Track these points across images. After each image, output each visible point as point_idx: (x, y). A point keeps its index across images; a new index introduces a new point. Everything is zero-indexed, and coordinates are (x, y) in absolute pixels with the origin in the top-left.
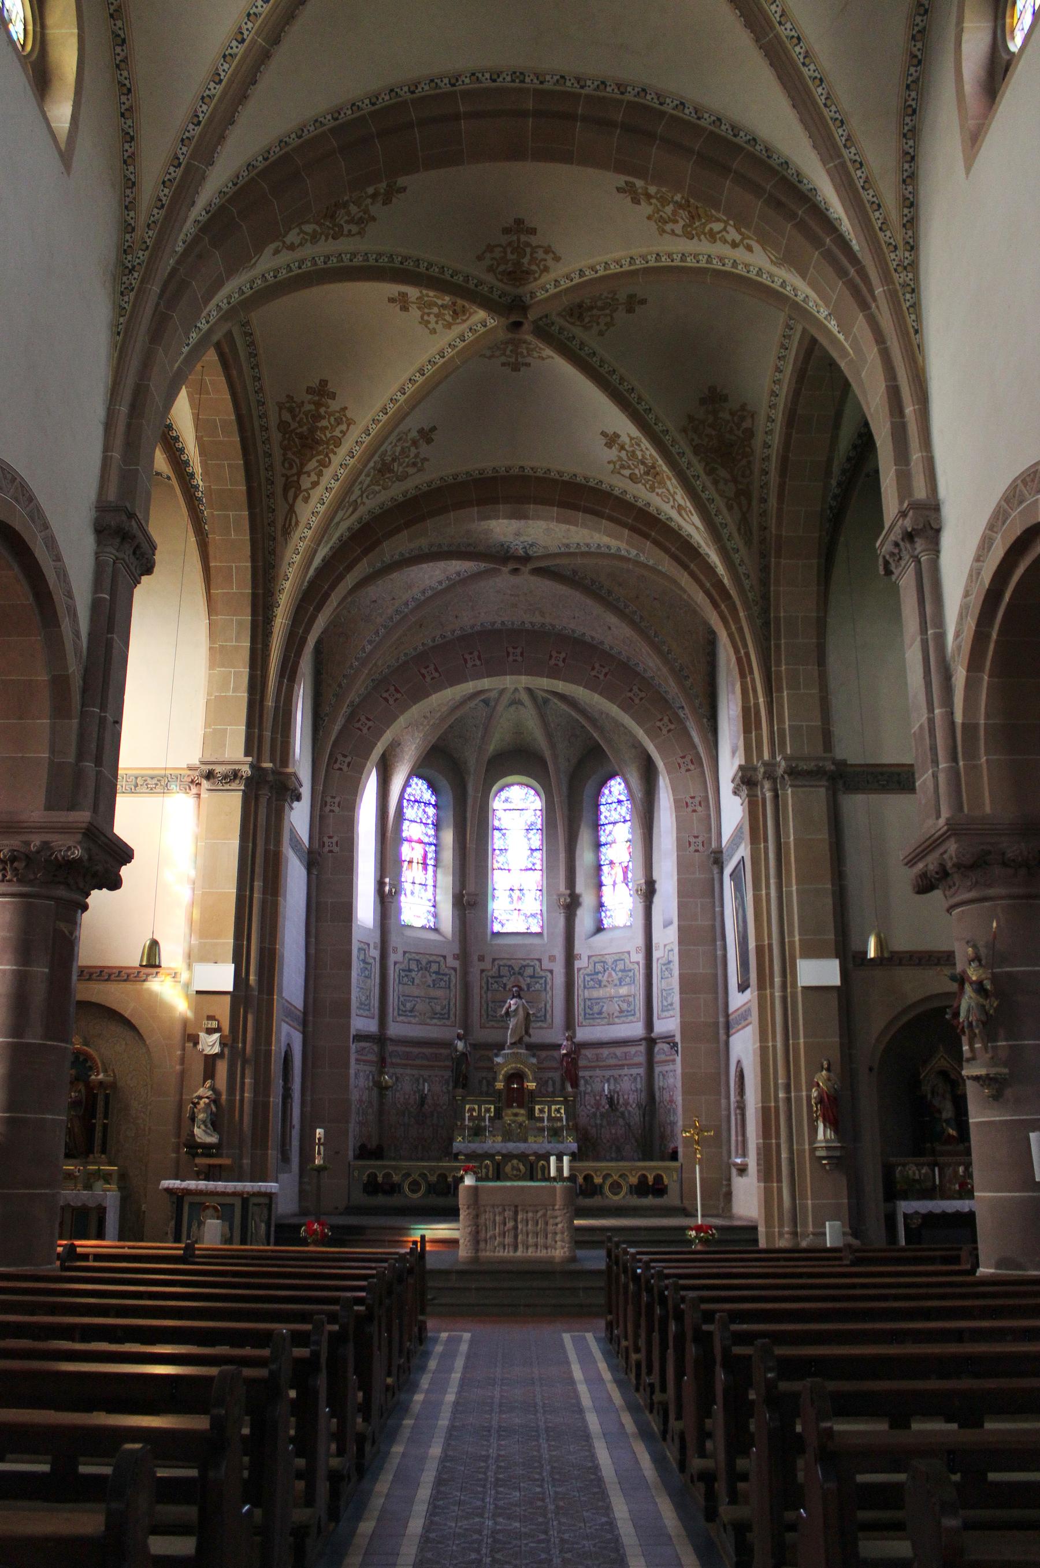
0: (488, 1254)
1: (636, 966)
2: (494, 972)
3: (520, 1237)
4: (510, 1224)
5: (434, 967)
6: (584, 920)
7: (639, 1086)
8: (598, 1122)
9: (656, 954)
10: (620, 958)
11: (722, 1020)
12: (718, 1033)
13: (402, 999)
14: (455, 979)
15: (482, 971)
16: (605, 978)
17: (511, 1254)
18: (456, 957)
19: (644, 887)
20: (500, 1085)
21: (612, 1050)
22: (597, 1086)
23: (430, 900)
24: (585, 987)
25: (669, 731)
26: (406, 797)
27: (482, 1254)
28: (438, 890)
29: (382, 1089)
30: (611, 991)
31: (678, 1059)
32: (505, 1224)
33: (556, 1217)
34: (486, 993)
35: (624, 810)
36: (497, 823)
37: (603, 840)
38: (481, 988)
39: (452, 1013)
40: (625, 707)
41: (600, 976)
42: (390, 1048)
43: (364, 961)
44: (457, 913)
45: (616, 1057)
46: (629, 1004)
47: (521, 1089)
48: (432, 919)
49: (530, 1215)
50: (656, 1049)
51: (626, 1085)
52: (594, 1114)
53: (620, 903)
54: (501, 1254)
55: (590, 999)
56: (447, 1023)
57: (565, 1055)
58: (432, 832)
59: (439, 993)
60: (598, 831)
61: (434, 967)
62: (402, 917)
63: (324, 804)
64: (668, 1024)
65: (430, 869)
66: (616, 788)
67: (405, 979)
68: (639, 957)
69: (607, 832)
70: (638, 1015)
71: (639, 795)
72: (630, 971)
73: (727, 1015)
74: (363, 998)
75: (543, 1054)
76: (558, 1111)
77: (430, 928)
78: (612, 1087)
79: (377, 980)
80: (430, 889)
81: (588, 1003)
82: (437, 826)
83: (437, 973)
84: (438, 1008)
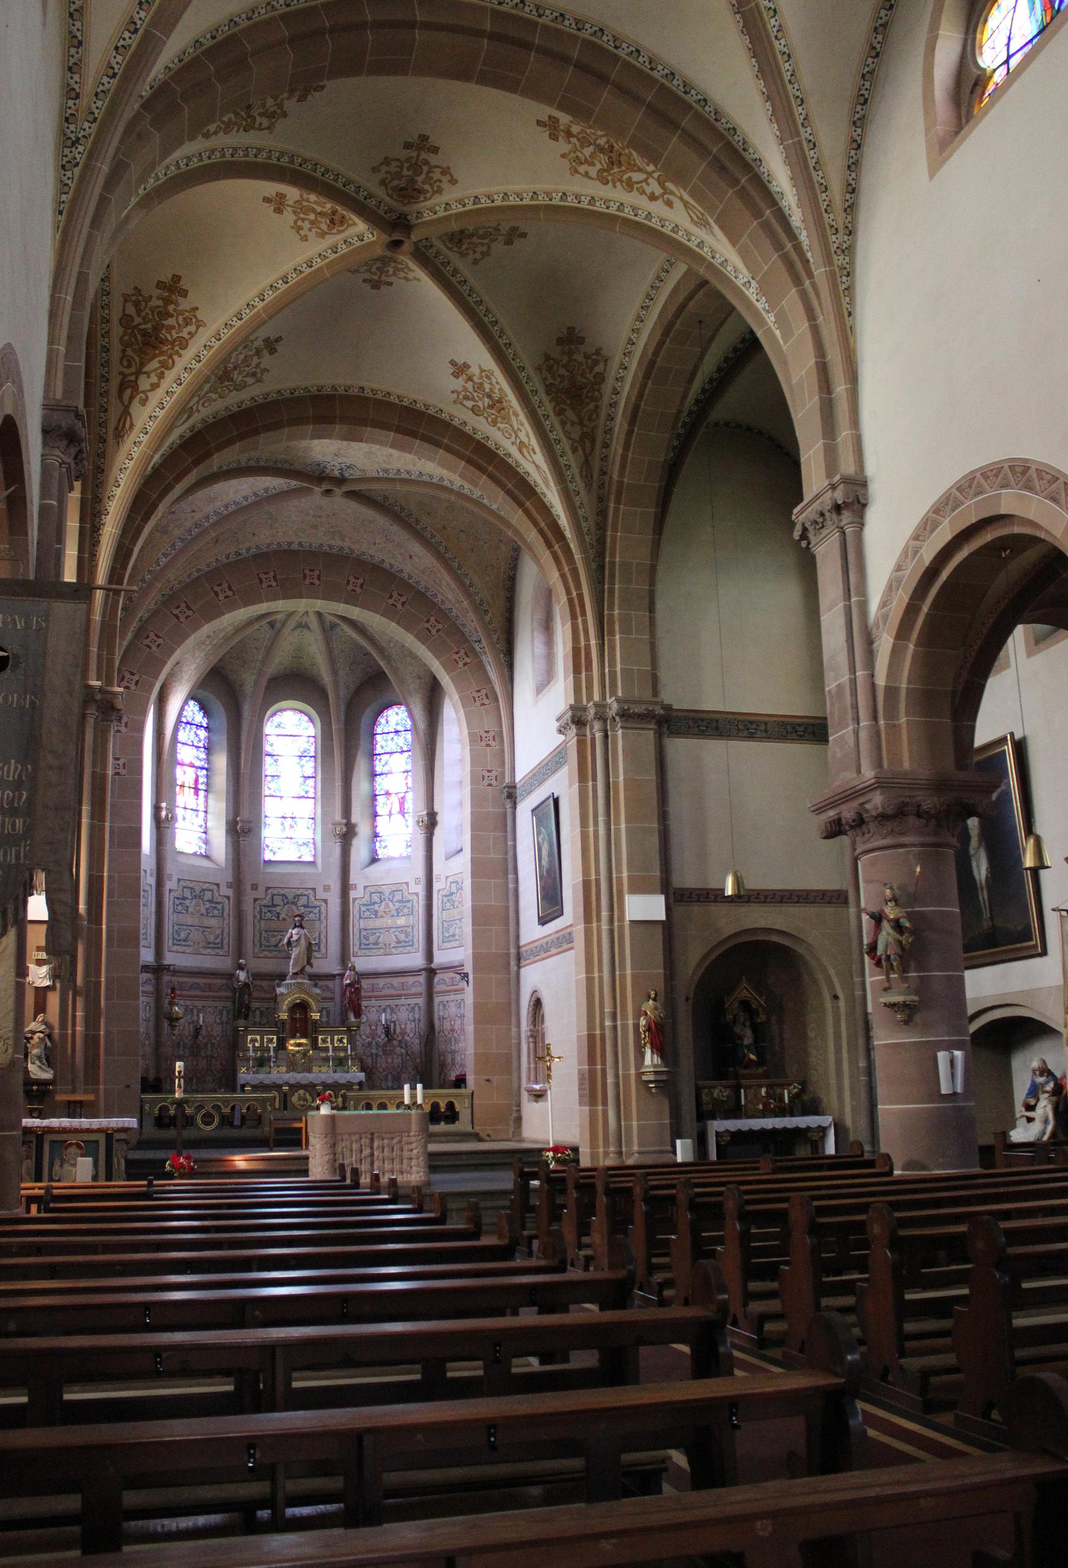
2: (267, 901)
4: (367, 1152)
5: (208, 895)
6: (360, 850)
7: (417, 1016)
8: (374, 1051)
9: (436, 886)
10: (397, 888)
11: (513, 951)
12: (509, 964)
14: (229, 908)
15: (255, 900)
18: (229, 885)
20: (284, 1016)
21: (389, 980)
23: (201, 826)
24: (360, 918)
25: (465, 664)
28: (209, 817)
30: (388, 921)
31: (469, 990)
32: (361, 1151)
35: (405, 739)
37: (379, 769)
38: (255, 917)
39: (225, 942)
40: (424, 637)
41: (376, 907)
44: (230, 840)
45: (393, 987)
46: (407, 935)
49: (386, 1141)
50: (436, 980)
51: (403, 1015)
52: (370, 1044)
58: (203, 756)
59: (212, 922)
61: (208, 895)
66: (395, 718)
69: (383, 762)
71: (422, 726)
72: (408, 901)
73: (518, 947)
76: (340, 1040)
78: (389, 1017)
79: (153, 909)
80: (202, 815)
81: (364, 933)
83: (211, 901)
84: (211, 938)
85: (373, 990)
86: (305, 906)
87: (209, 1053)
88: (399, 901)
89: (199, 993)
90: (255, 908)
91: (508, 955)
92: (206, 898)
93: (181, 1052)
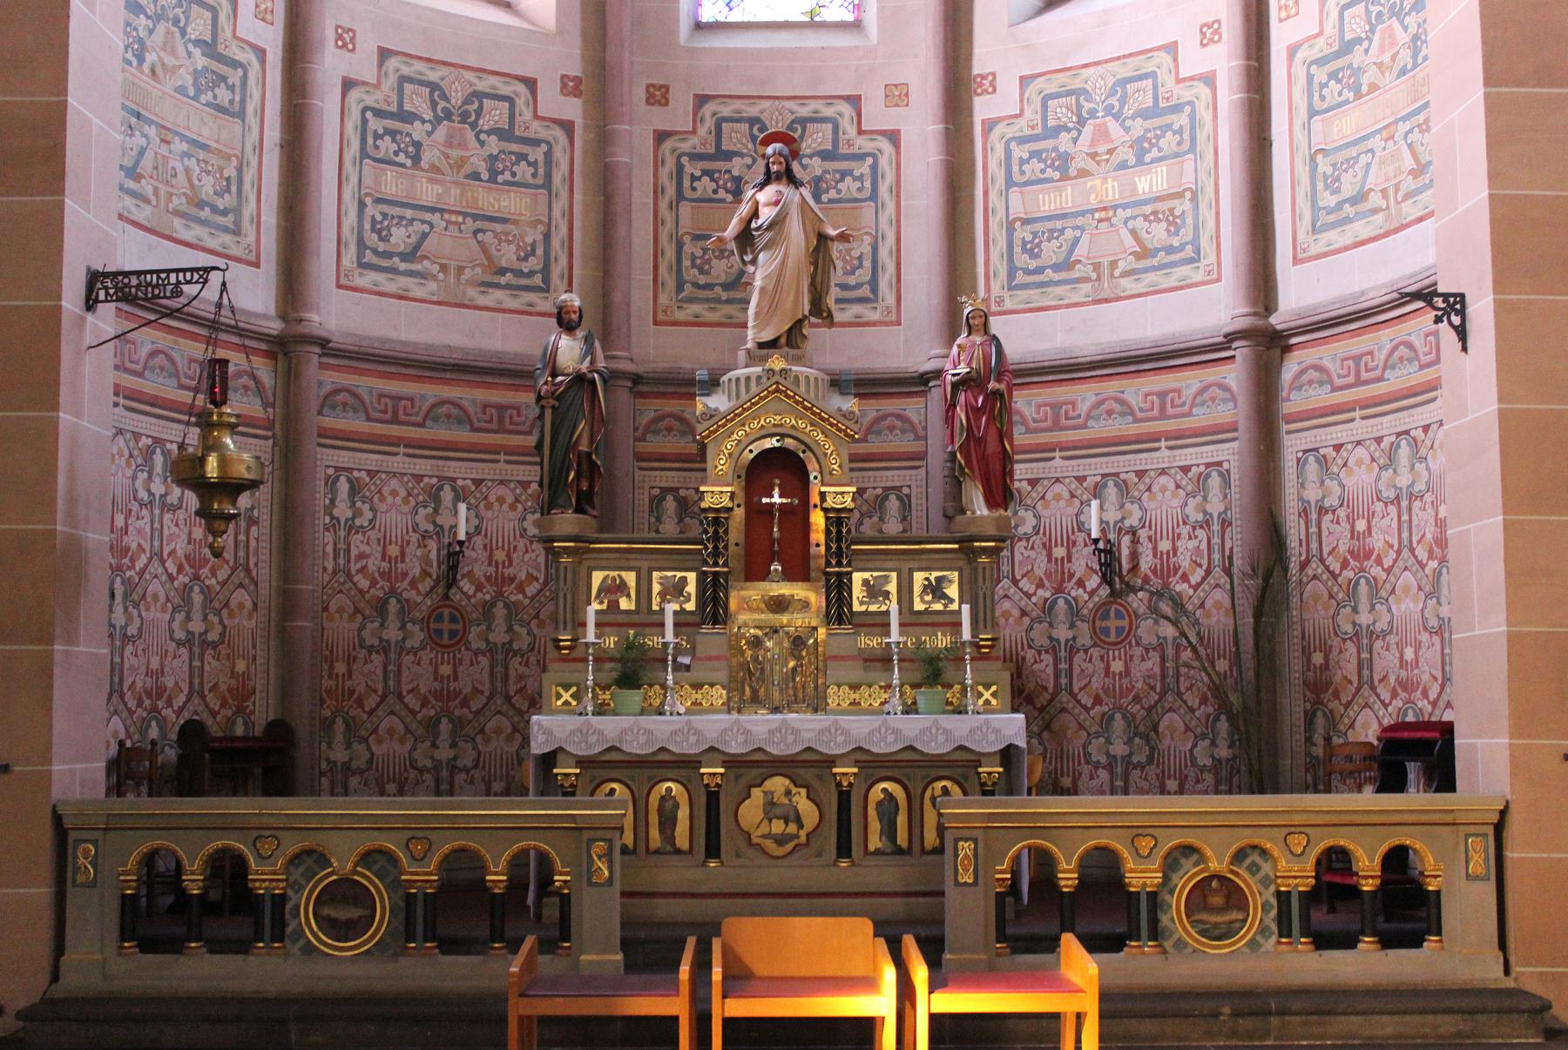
1: (1203, 90)
24: (1010, 182)
88: (1144, 114)
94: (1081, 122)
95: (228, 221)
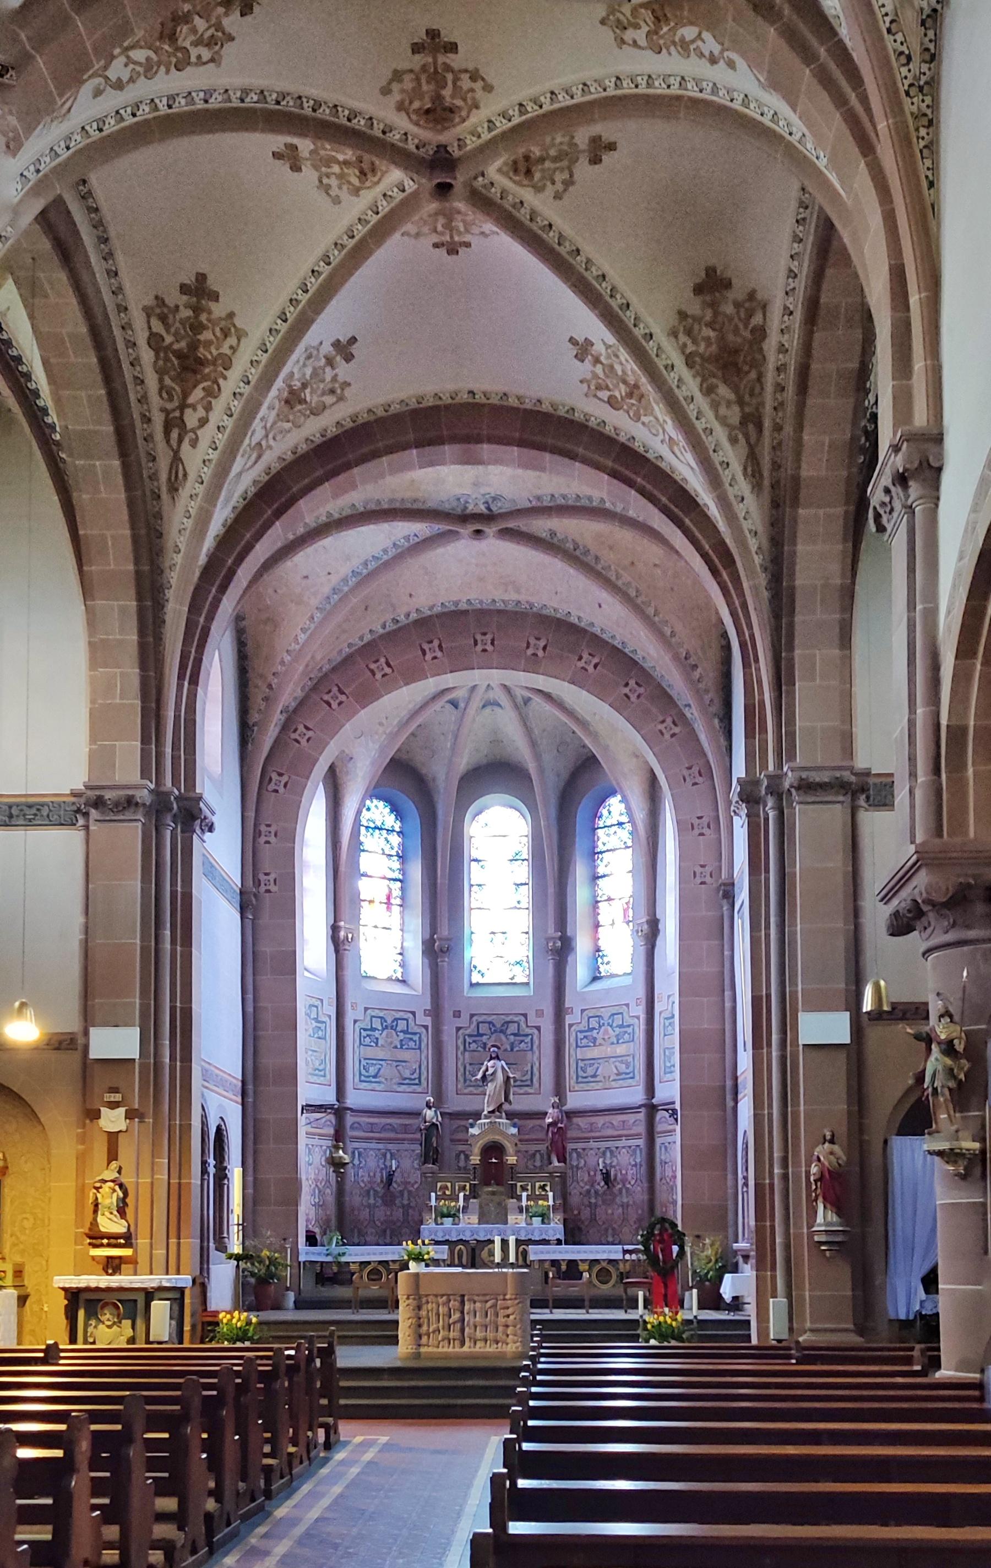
0: (430, 1349)
1: (636, 1020)
3: (467, 1330)
4: (456, 1316)
5: (402, 1025)
7: (638, 1160)
8: (593, 1200)
9: (658, 1008)
13: (364, 1062)
15: (458, 1029)
16: (601, 1035)
17: (457, 1350)
19: (645, 927)
20: (475, 1159)
21: (607, 1118)
22: (592, 1161)
24: (577, 1046)
26: (364, 822)
27: (423, 1350)
29: (336, 1164)
30: (609, 1050)
31: (678, 1128)
32: (450, 1317)
33: (508, 1308)
34: (463, 1054)
35: (625, 834)
36: (474, 854)
37: (601, 870)
42: (350, 1119)
43: (317, 1020)
44: (426, 961)
45: (613, 1126)
47: (502, 1163)
48: (400, 970)
49: (478, 1305)
50: (658, 1118)
51: (624, 1159)
52: (588, 1192)
53: (618, 947)
54: (445, 1349)
55: (582, 1060)
56: (418, 1089)
57: (550, 1125)
58: (396, 865)
60: (594, 861)
61: (402, 1025)
62: (364, 968)
63: (257, 834)
64: (669, 1089)
65: (396, 910)
67: (368, 1039)
68: (640, 1011)
70: (637, 1078)
74: (317, 1063)
75: (531, 1123)
76: (543, 1188)
77: (398, 980)
78: (608, 1162)
82: (402, 858)
84: (407, 1074)
85: (591, 1131)
86: (515, 1035)
87: (406, 1202)
88: (621, 1026)
89: (392, 1135)
90: (457, 1038)
91: (724, 1087)
92: (399, 1029)
93: (372, 1201)
94: (600, 1027)
95: (322, 1073)
